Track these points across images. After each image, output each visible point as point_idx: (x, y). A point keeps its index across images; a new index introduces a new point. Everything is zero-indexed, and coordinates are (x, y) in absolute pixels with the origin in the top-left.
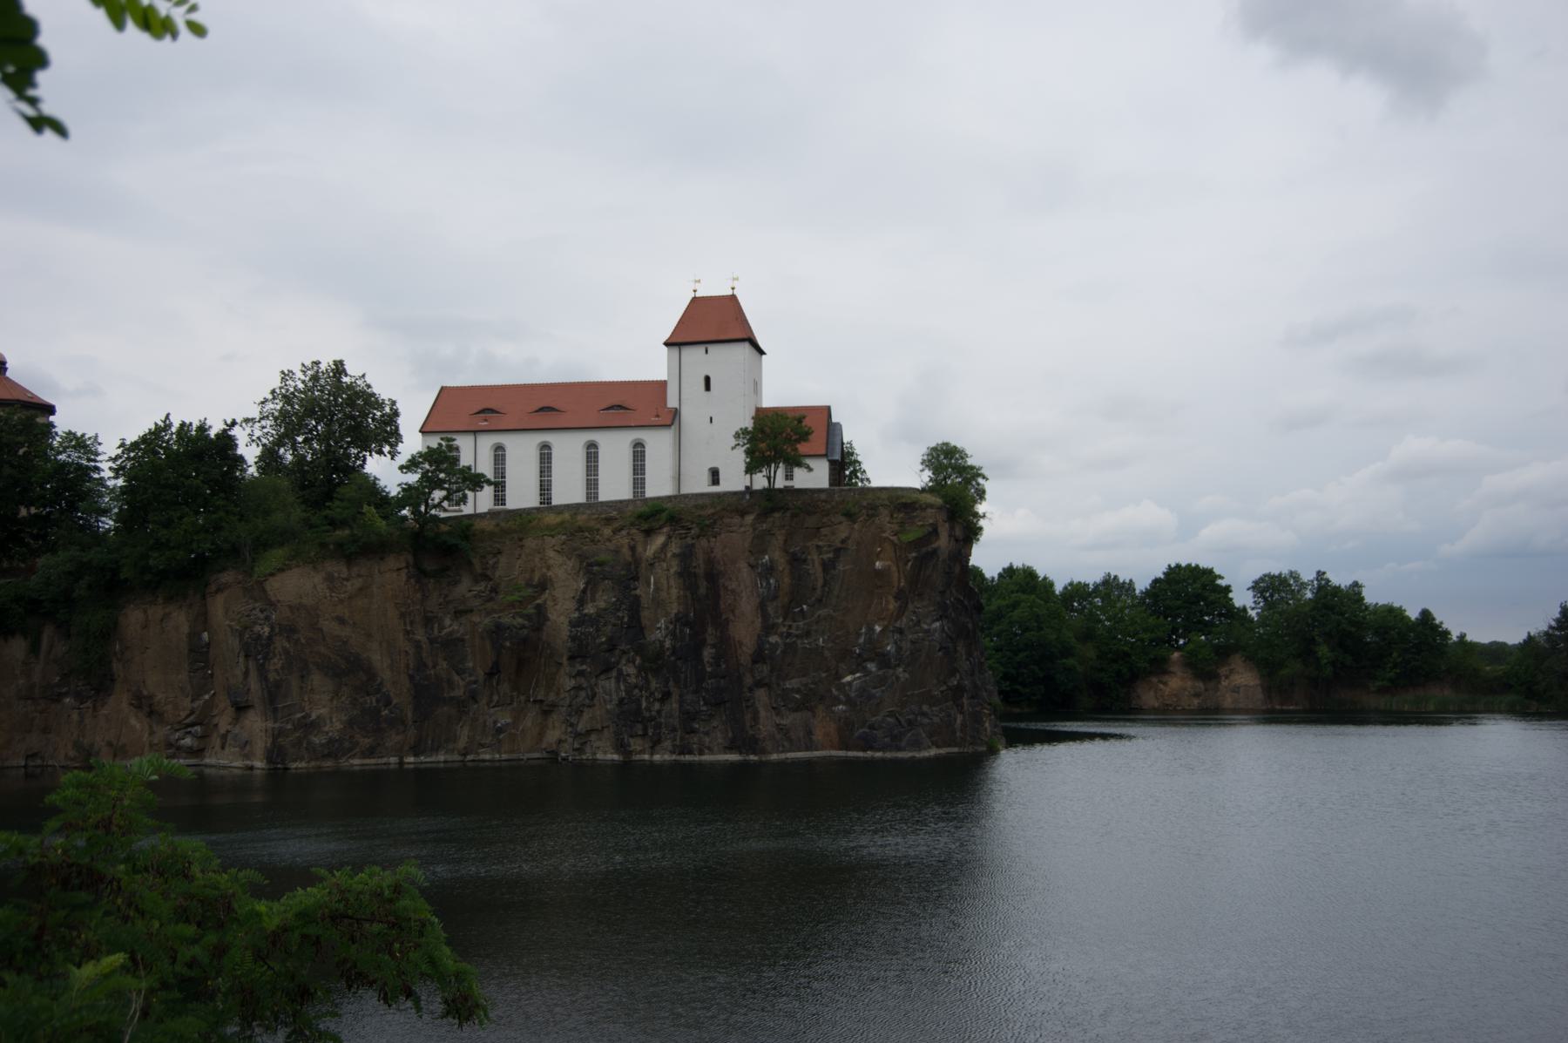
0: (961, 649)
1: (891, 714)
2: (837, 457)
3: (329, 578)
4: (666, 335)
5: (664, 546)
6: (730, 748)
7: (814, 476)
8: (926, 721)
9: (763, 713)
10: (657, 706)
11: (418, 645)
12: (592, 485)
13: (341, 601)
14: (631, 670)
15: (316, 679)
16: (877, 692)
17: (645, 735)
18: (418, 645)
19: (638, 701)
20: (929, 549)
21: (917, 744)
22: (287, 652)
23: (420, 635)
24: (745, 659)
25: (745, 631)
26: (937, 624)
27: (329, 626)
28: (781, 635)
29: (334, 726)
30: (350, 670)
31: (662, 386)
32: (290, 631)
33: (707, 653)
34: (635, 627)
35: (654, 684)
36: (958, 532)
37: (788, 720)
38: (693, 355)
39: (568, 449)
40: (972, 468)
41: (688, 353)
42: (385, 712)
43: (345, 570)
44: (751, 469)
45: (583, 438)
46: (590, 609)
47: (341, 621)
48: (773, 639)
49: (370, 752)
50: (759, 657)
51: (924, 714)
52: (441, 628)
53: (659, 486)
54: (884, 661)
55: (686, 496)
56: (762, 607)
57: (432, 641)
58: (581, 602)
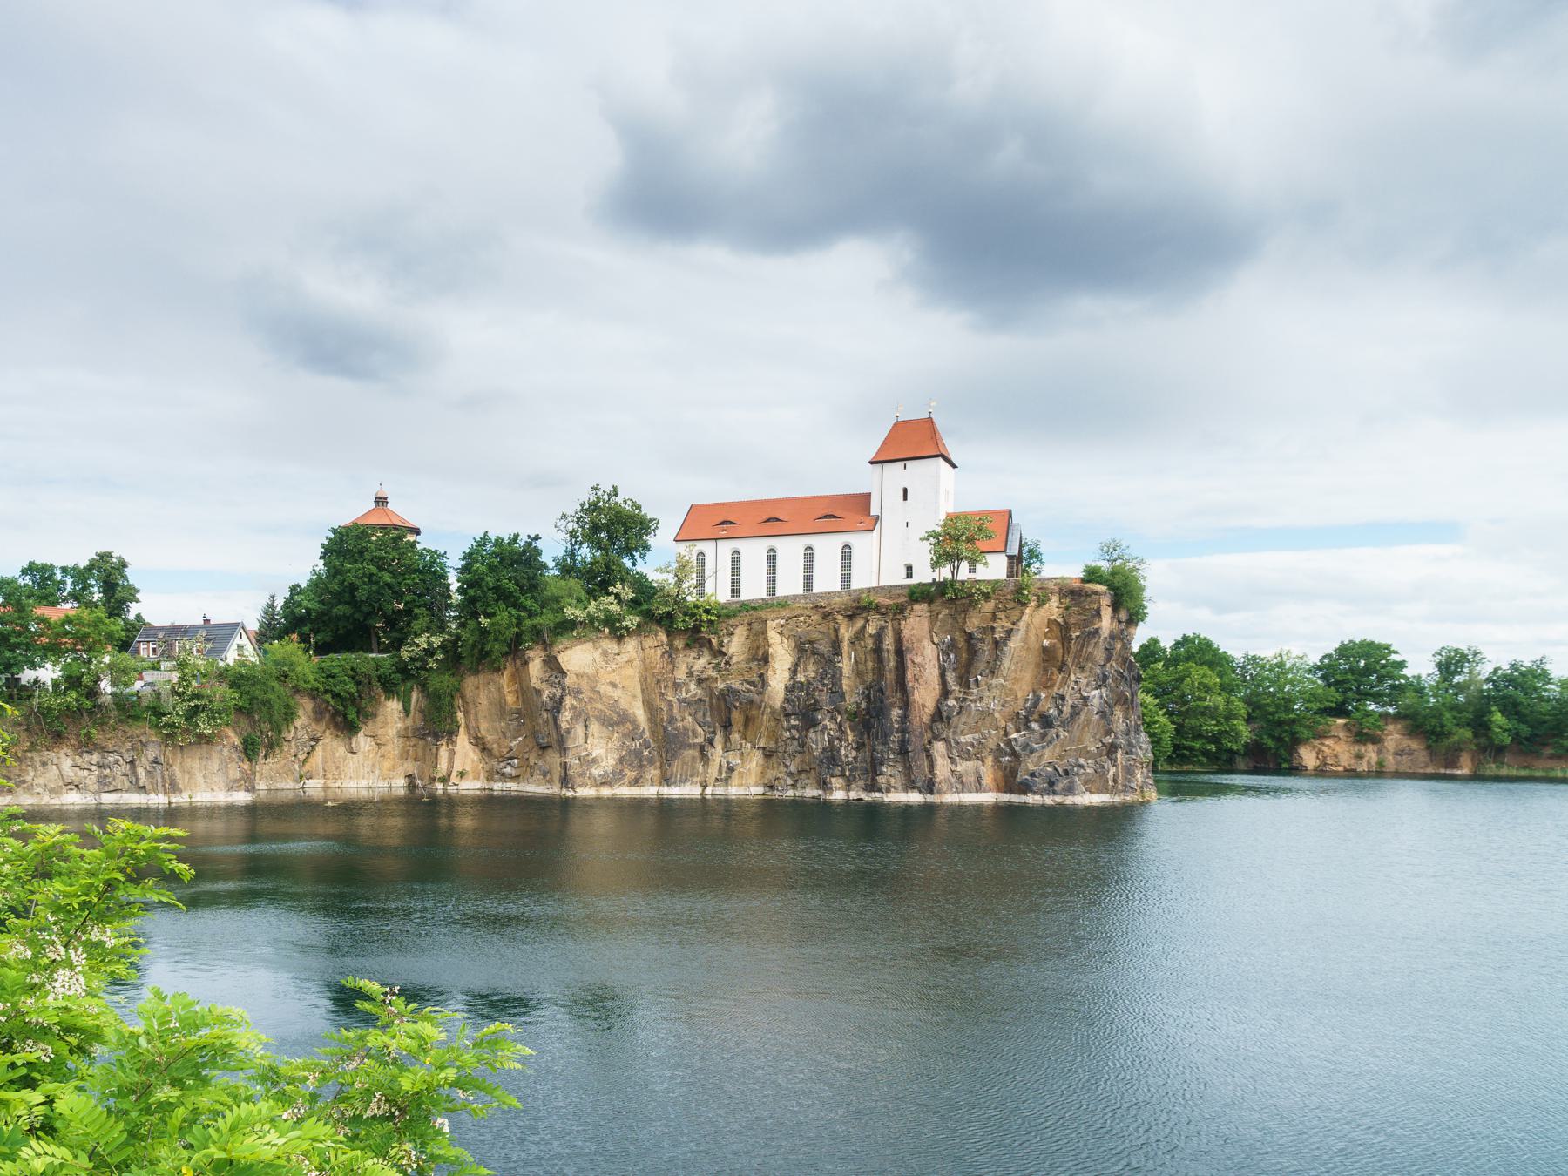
0: (1119, 713)
2: (1016, 553)
3: (605, 654)
4: (871, 456)
5: (864, 628)
6: (910, 786)
7: (994, 569)
10: (854, 753)
11: (670, 704)
12: (808, 580)
15: (595, 727)
17: (843, 776)
19: (839, 751)
20: (1091, 629)
21: (1070, 790)
22: (574, 707)
24: (926, 719)
25: (925, 696)
26: (1096, 692)
27: (603, 688)
28: (957, 699)
30: (616, 720)
31: (868, 496)
32: (577, 693)
34: (837, 693)
36: (1123, 615)
37: (963, 767)
38: (893, 470)
39: (790, 550)
41: (886, 466)
42: (646, 753)
44: (935, 565)
45: (799, 544)
46: (801, 678)
47: (614, 685)
50: (938, 716)
51: (1081, 766)
52: (688, 691)
53: (862, 580)
54: (1046, 722)
55: (882, 588)
56: (942, 676)
57: (680, 701)
58: (794, 672)
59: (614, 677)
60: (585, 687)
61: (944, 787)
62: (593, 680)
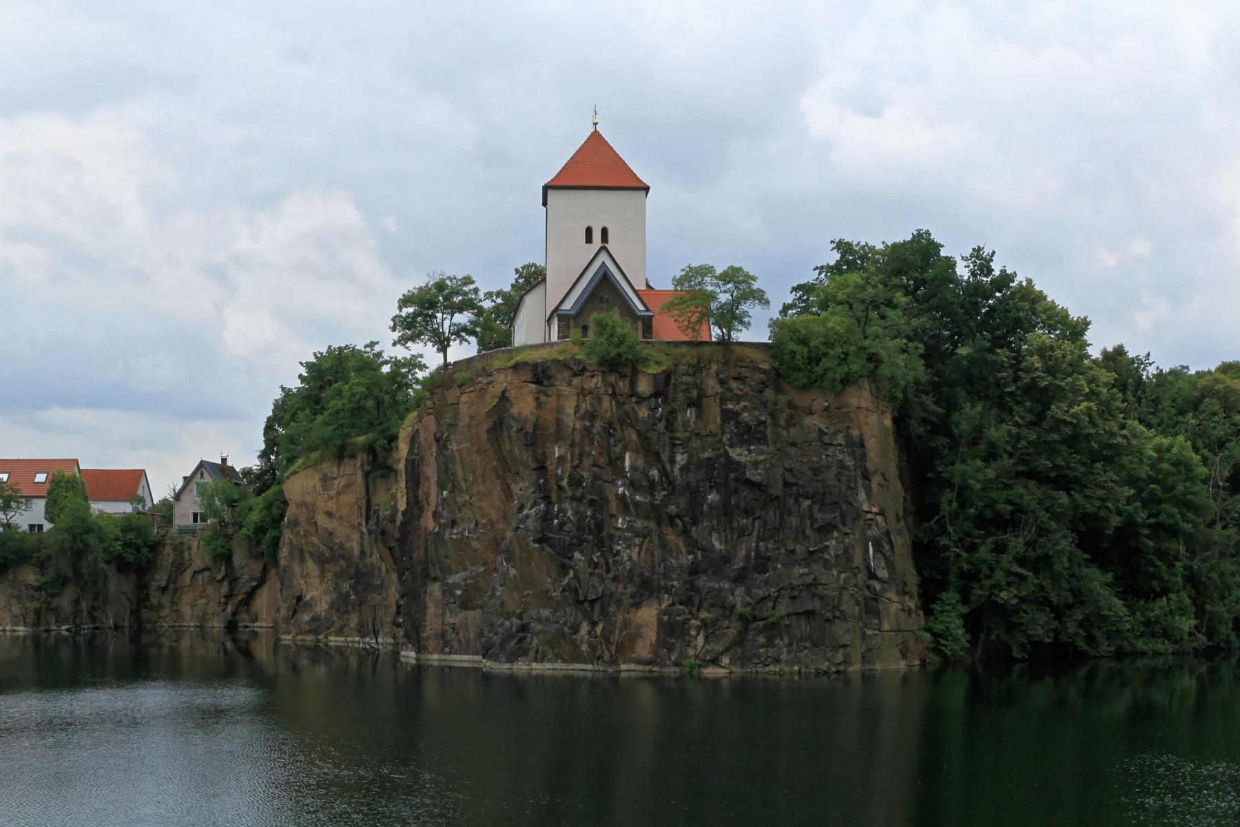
3: (326, 480)
8: (539, 627)
9: (431, 609)
13: (331, 498)
15: (311, 566)
27: (321, 519)
29: (322, 608)
43: (335, 469)
47: (330, 514)
49: (340, 632)
59: (331, 506)
60: (302, 519)
61: (431, 644)
62: (310, 509)
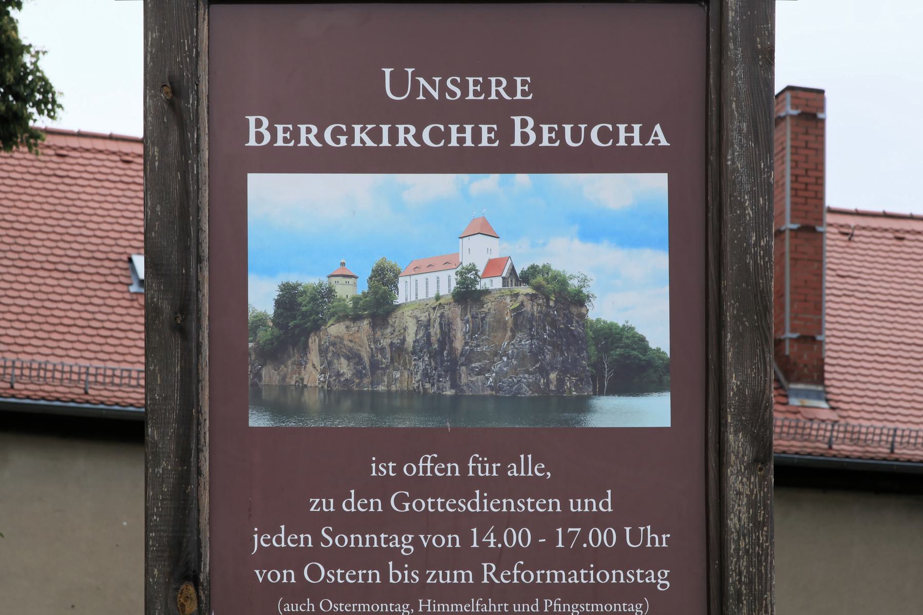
1: (511, 378)
9: (463, 376)
11: (372, 349)
14: (426, 359)
16: (505, 369)
18: (372, 349)
23: (372, 346)
25: (458, 345)
27: (345, 342)
30: (354, 357)
33: (445, 353)
34: (429, 342)
35: (433, 364)
40: (279, 303)
47: (351, 341)
48: (467, 348)
50: (462, 355)
56: (464, 335)
